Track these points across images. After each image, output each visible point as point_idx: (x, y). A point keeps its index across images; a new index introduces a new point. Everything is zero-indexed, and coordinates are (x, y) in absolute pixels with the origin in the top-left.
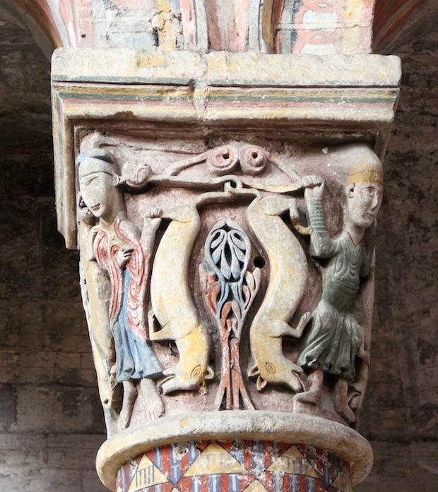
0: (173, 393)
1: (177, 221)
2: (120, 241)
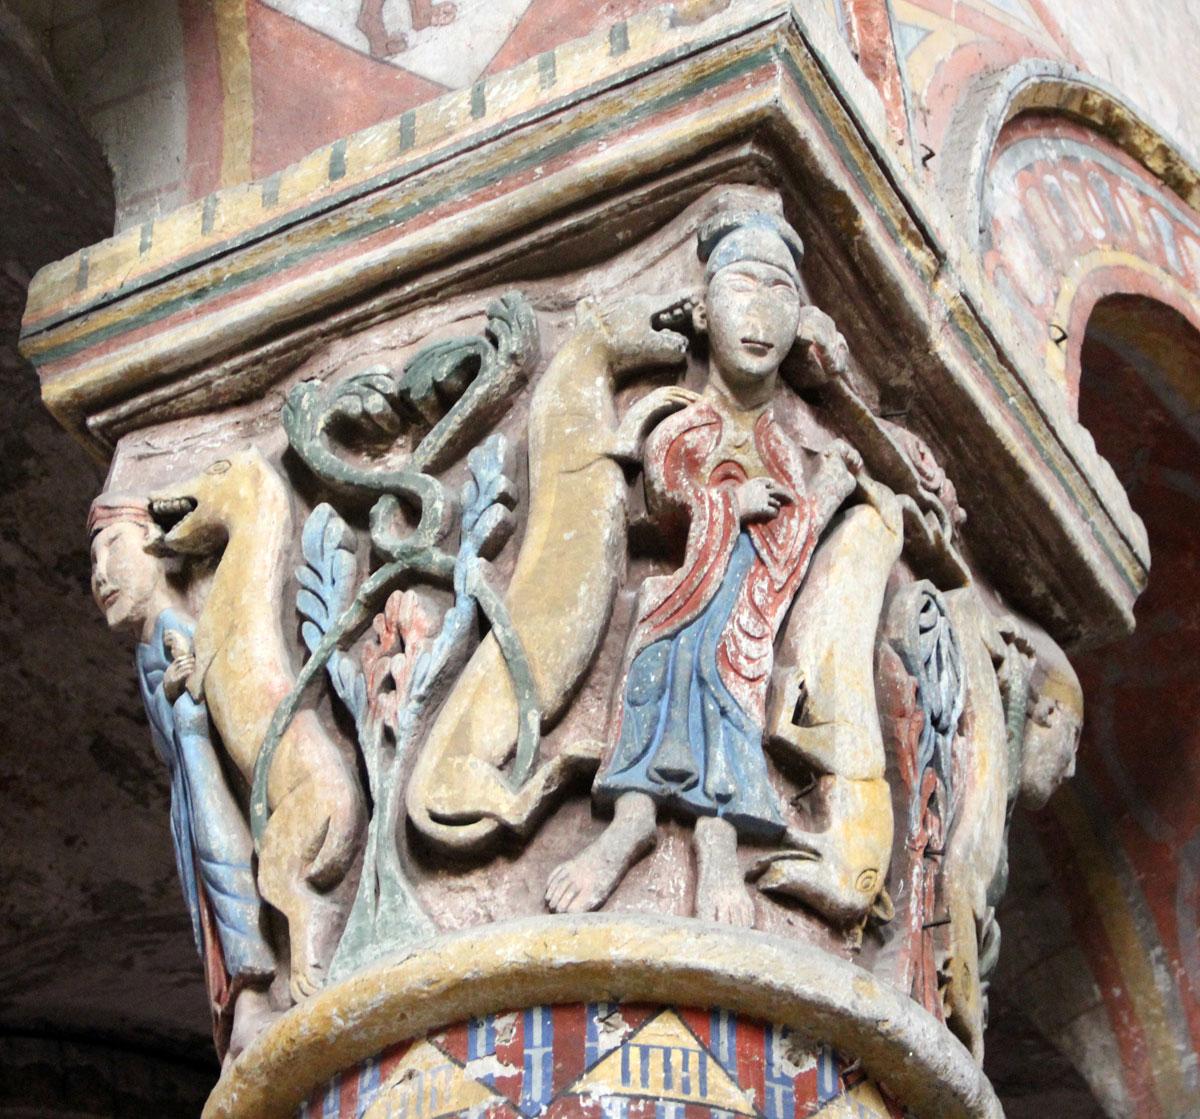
0: (791, 899)
1: (878, 511)
2: (760, 464)
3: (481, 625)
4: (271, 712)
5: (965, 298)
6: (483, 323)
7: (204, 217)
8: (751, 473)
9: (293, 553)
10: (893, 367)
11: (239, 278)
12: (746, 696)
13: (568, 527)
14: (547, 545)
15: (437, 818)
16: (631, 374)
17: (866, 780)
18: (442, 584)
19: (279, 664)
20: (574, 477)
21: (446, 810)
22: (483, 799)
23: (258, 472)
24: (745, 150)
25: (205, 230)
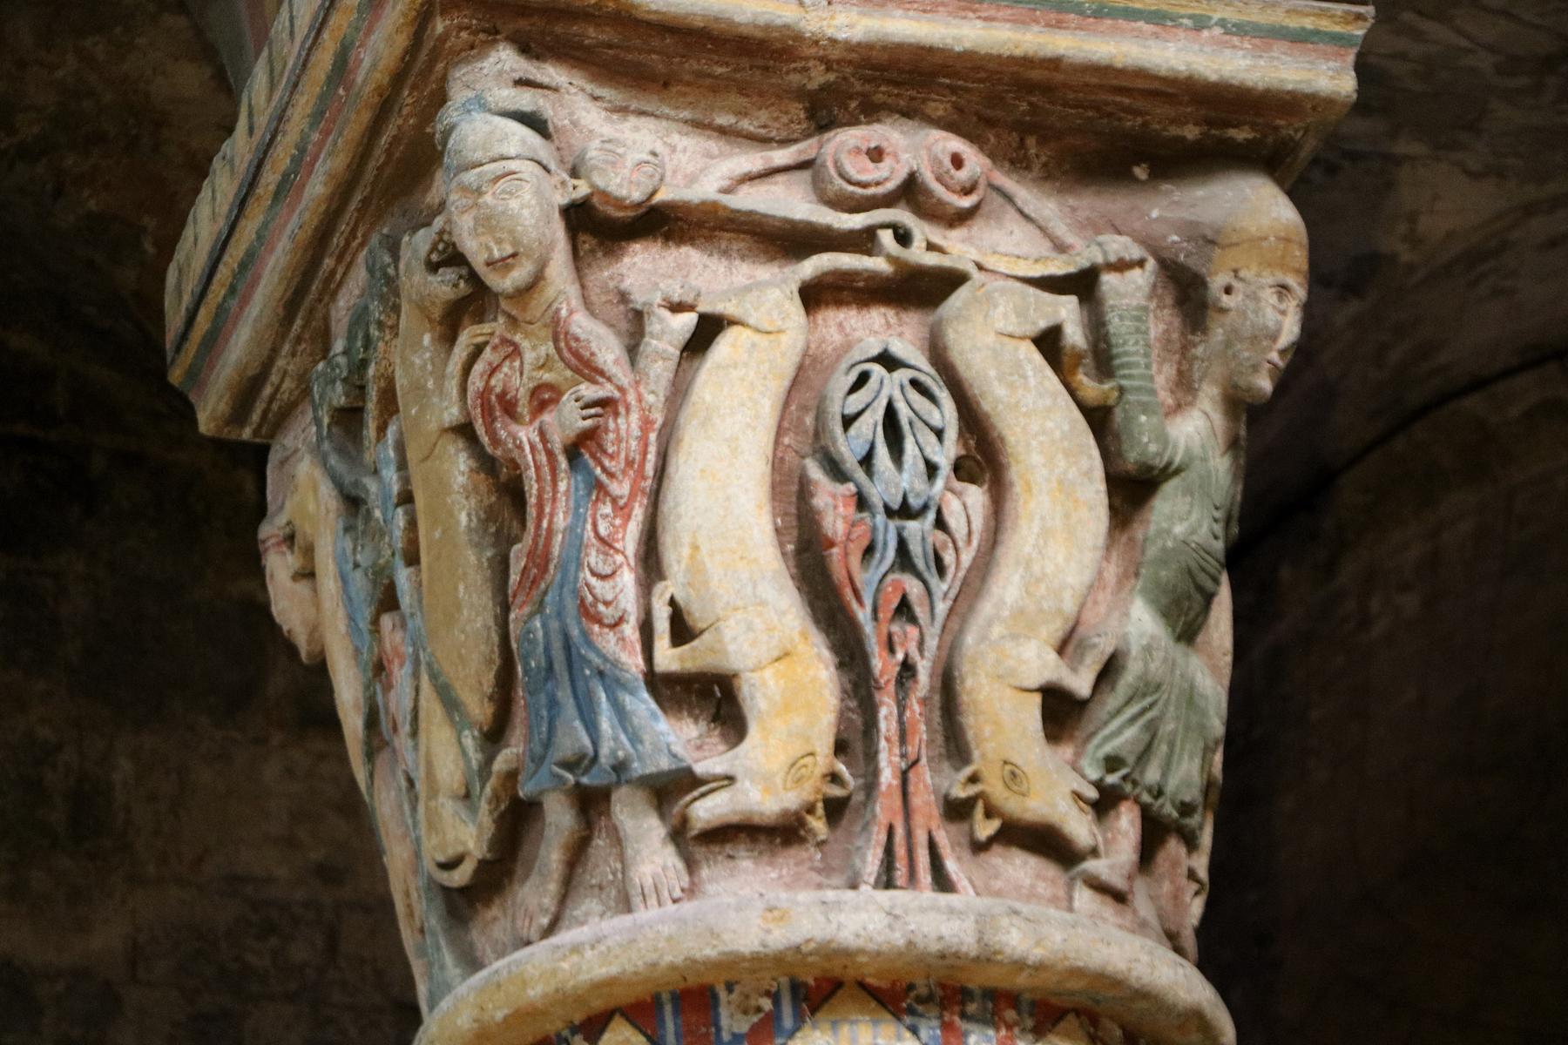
0: (725, 835)
2: (569, 373)
8: (564, 388)
11: (243, 266)
17: (778, 659)
24: (440, 25)
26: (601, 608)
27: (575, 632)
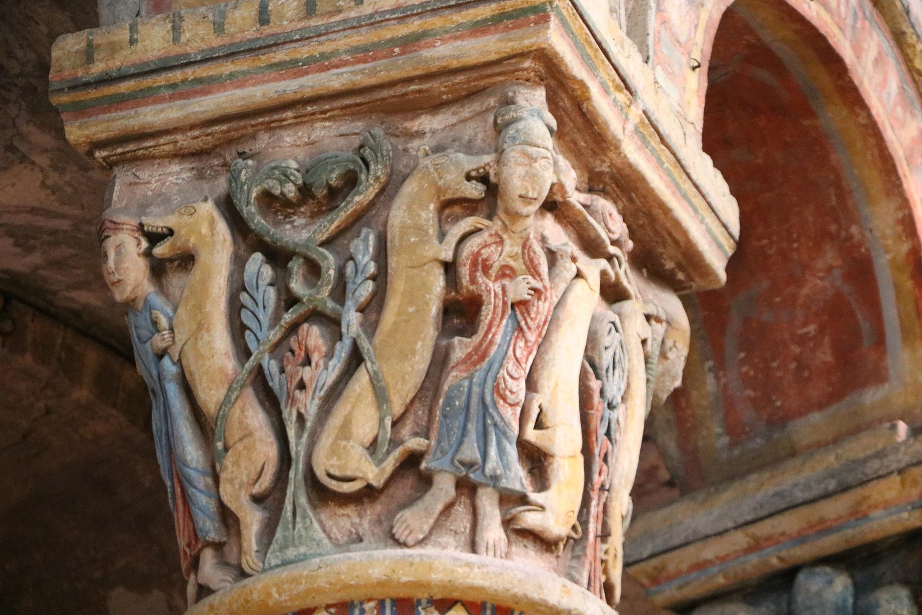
2: (524, 267)
3: (356, 359)
4: (227, 386)
5: (644, 112)
6: (357, 141)
7: (173, 28)
8: (518, 273)
9: (238, 288)
10: (598, 162)
11: (199, 81)
12: (511, 416)
13: (411, 303)
14: (399, 314)
15: (330, 476)
16: (452, 207)
17: (571, 457)
18: (332, 324)
19: (231, 354)
20: (415, 271)
21: (337, 473)
22: (358, 469)
23: (213, 217)
25: (176, 40)
26: (508, 393)
27: (488, 399)
